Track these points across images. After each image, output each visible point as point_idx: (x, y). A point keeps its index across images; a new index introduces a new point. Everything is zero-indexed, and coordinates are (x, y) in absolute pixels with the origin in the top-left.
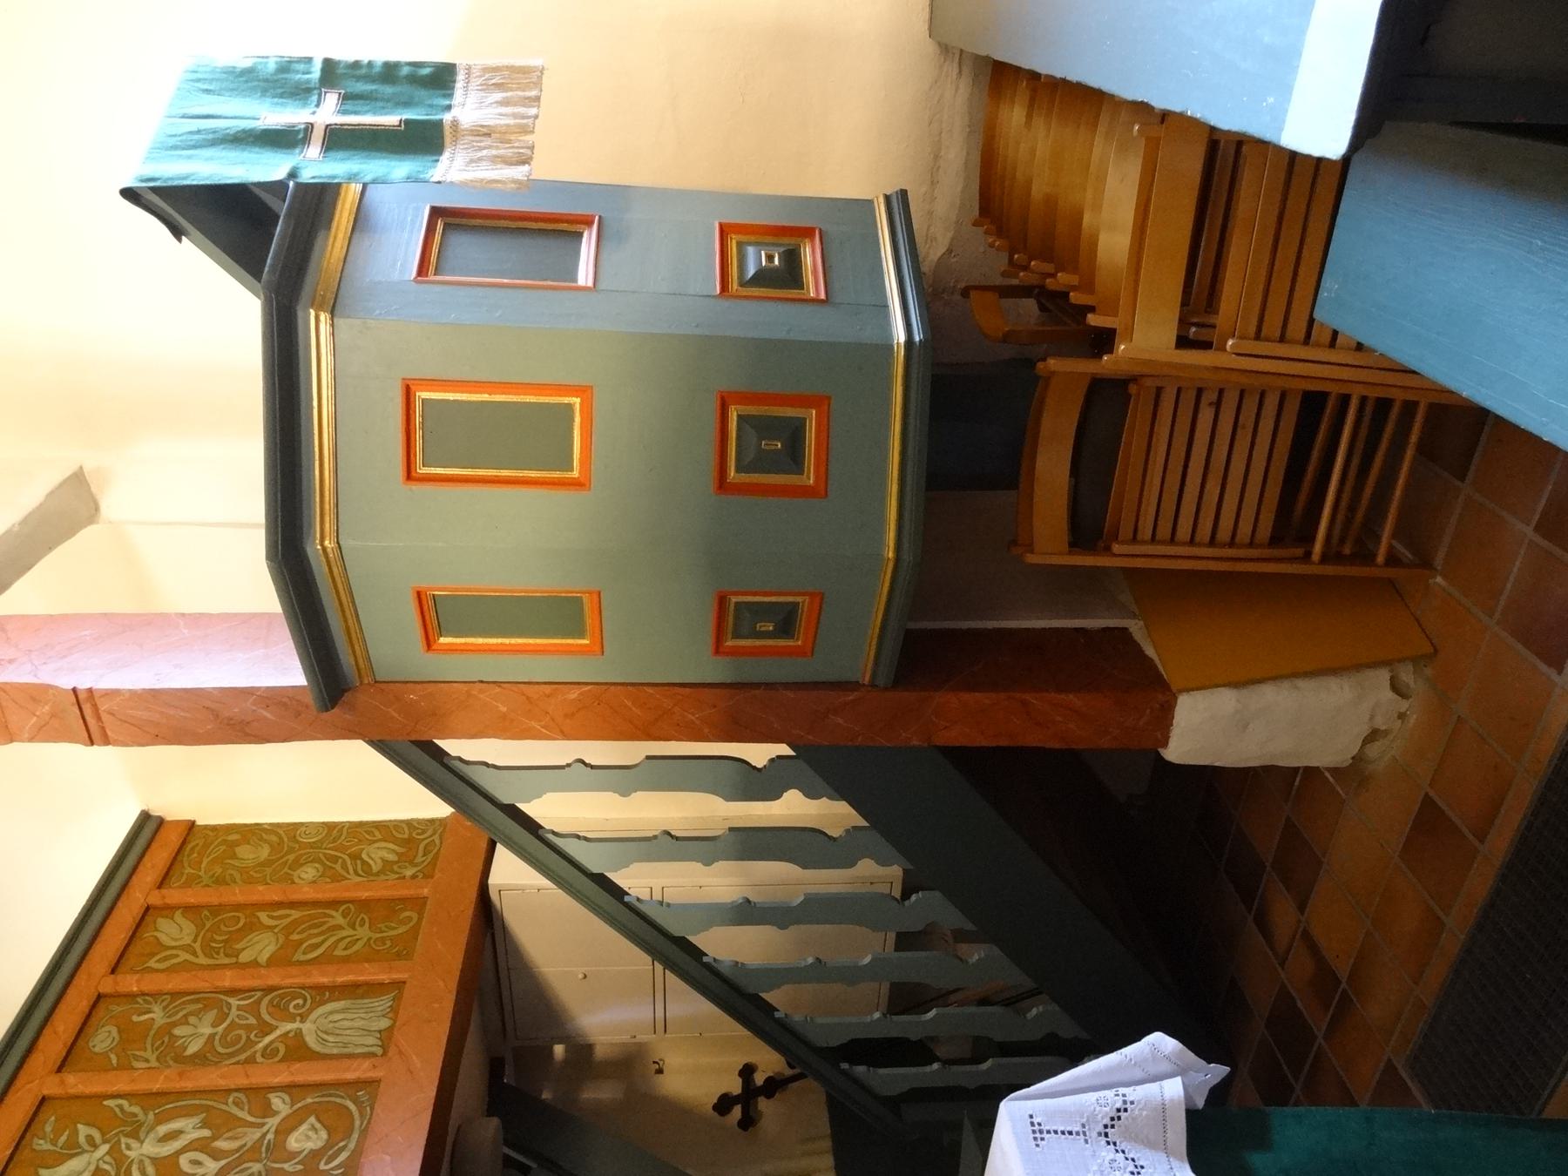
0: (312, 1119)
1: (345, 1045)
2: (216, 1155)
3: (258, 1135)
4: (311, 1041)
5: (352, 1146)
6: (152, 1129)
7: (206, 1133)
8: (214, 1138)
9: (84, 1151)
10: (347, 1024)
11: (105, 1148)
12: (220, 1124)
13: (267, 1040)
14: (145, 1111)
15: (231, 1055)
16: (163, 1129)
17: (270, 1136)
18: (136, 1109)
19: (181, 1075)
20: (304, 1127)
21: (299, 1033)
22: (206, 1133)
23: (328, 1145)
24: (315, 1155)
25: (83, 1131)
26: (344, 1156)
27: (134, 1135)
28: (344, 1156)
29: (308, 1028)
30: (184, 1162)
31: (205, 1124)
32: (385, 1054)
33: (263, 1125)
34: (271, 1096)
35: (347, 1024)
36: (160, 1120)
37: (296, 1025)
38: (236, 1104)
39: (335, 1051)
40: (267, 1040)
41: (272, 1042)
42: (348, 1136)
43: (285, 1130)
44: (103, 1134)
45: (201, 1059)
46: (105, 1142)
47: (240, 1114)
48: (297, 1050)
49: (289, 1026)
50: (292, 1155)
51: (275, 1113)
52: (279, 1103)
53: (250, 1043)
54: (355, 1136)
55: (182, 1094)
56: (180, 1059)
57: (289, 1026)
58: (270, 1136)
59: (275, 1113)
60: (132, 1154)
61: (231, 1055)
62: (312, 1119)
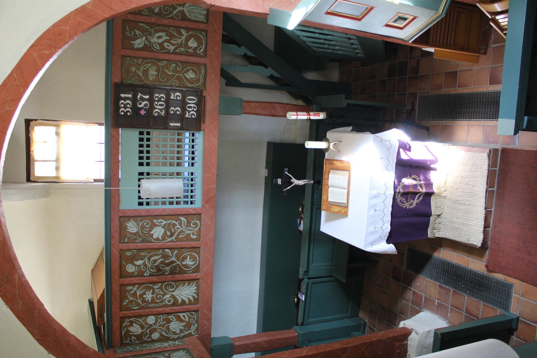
0: (193, 38)
1: (196, 17)
2: (173, 45)
3: (181, 41)
4: (187, 14)
5: (204, 47)
6: (154, 34)
7: (168, 38)
8: (171, 40)
9: (139, 38)
10: (196, 11)
11: (144, 38)
12: (172, 36)
13: (176, 11)
14: (151, 28)
15: (167, 15)
16: (157, 35)
17: (184, 42)
18: (148, 27)
19: (157, 19)
20: (191, 40)
21: (183, 11)
22: (168, 38)
23: (198, 47)
24: (195, 49)
25: (137, 32)
26: (202, 50)
27: (150, 35)
28: (202, 50)
29: (185, 9)
30: (165, 44)
31: (167, 35)
32: (207, 23)
33: (181, 38)
34: (181, 30)
35: (196, 11)
36: (156, 31)
37: (181, 8)
38: (173, 31)
39: (194, 19)
40: (176, 11)
41: (177, 13)
42: (202, 45)
43: (188, 39)
44: (143, 34)
45: (158, 14)
46: (144, 36)
47: (175, 34)
48: (184, 18)
49: (179, 8)
50: (190, 48)
51: (183, 35)
52: (183, 32)
53: (171, 12)
54: (204, 45)
55: (159, 25)
56: (153, 13)
57: (179, 8)
58: (184, 42)
59: (183, 35)
60: (152, 41)
61: (167, 15)
62: (193, 38)
